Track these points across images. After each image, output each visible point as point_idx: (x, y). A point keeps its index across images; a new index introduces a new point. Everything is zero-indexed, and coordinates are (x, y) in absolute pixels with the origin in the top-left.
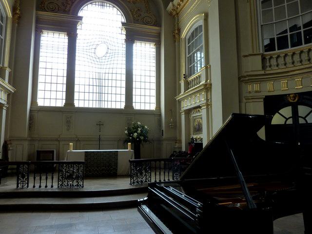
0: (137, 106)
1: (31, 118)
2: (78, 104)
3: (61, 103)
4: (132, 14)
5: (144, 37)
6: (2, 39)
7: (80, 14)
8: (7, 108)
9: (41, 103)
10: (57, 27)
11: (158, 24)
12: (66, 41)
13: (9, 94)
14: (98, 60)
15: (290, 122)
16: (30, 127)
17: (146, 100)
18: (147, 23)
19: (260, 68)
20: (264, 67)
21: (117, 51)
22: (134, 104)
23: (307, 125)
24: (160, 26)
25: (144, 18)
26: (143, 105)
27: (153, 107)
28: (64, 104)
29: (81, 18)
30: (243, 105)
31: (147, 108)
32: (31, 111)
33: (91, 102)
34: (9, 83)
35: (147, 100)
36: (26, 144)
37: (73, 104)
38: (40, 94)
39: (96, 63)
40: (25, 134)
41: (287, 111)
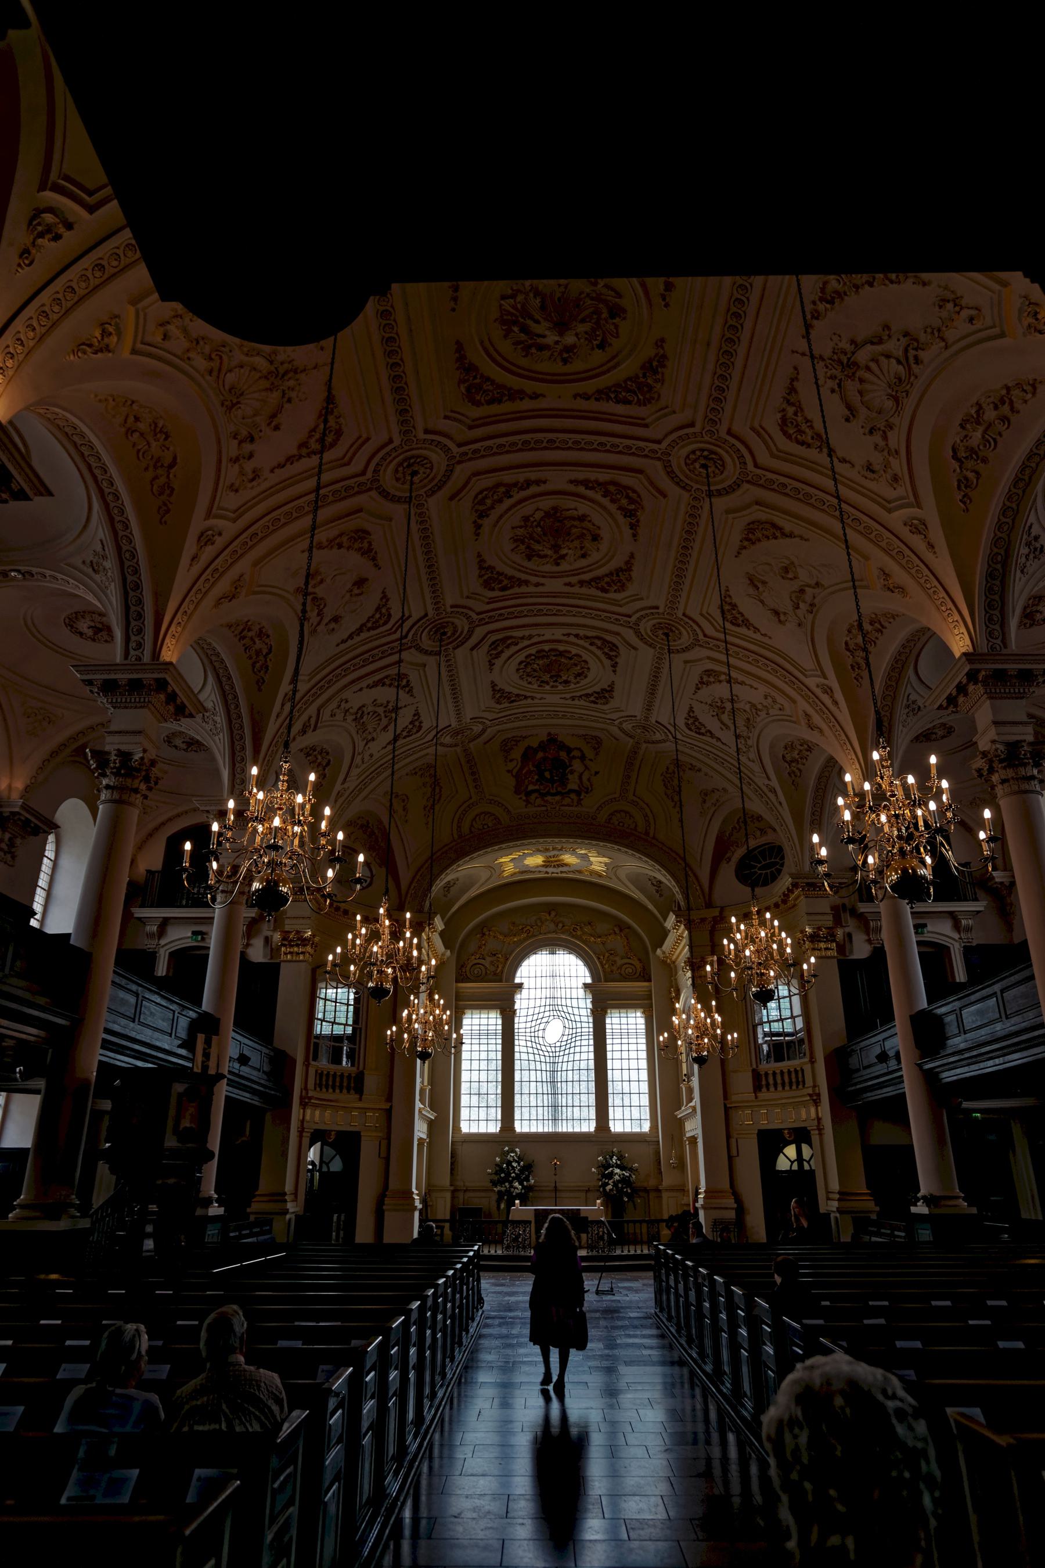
0: (616, 1127)
3: (494, 1128)
4: (601, 963)
5: (625, 1003)
7: (517, 981)
9: (465, 1128)
10: (483, 1003)
11: (645, 976)
12: (500, 1021)
13: (431, 1124)
14: (549, 1049)
15: (795, 1167)
16: (452, 1170)
17: (632, 1114)
18: (625, 978)
19: (751, 1089)
20: (757, 1088)
21: (579, 1030)
23: (812, 1172)
24: (650, 980)
25: (620, 968)
26: (628, 1123)
27: (646, 1127)
28: (498, 1129)
29: (520, 986)
30: (733, 1141)
31: (636, 1130)
33: (540, 1123)
35: (636, 1115)
36: (448, 1195)
37: (513, 1129)
38: (464, 1113)
39: (546, 1054)
40: (446, 1181)
41: (791, 1151)
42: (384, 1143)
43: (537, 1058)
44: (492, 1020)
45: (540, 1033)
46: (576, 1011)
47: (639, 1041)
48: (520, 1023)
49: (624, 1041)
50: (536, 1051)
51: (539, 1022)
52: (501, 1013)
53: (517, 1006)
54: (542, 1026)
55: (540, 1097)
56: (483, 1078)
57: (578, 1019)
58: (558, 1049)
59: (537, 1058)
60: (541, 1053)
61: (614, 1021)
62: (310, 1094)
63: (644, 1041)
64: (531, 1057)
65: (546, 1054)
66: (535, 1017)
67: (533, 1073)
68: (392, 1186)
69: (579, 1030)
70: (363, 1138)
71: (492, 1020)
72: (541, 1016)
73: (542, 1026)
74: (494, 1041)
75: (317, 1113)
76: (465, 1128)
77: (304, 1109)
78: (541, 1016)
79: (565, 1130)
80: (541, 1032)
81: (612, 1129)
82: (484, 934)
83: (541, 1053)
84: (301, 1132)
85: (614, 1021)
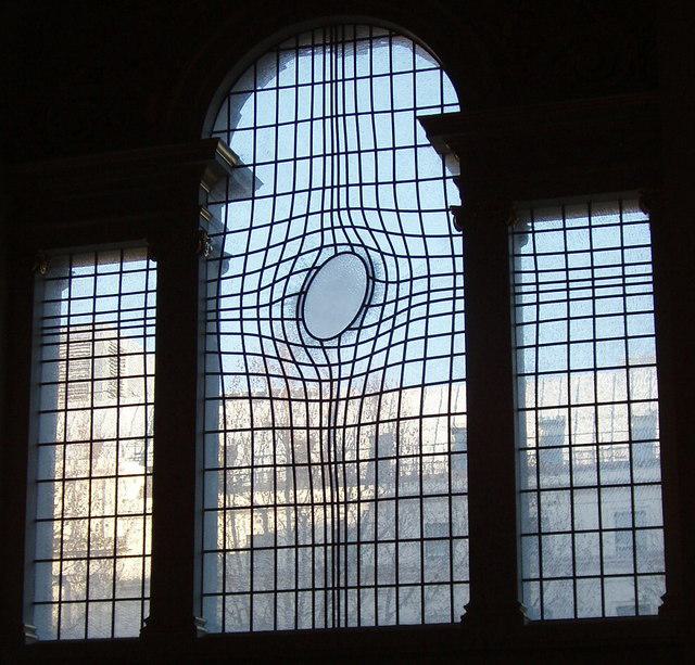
14: (319, 357)
21: (420, 285)
22: (531, 597)
46: (411, 224)
47: (633, 304)
49: (580, 308)
57: (416, 247)
58: (347, 354)
61: (550, 246)
63: (648, 303)
65: (309, 372)
69: (420, 285)
73: (296, 283)
74: (137, 345)
79: (368, 621)
81: (532, 612)
85: (550, 246)
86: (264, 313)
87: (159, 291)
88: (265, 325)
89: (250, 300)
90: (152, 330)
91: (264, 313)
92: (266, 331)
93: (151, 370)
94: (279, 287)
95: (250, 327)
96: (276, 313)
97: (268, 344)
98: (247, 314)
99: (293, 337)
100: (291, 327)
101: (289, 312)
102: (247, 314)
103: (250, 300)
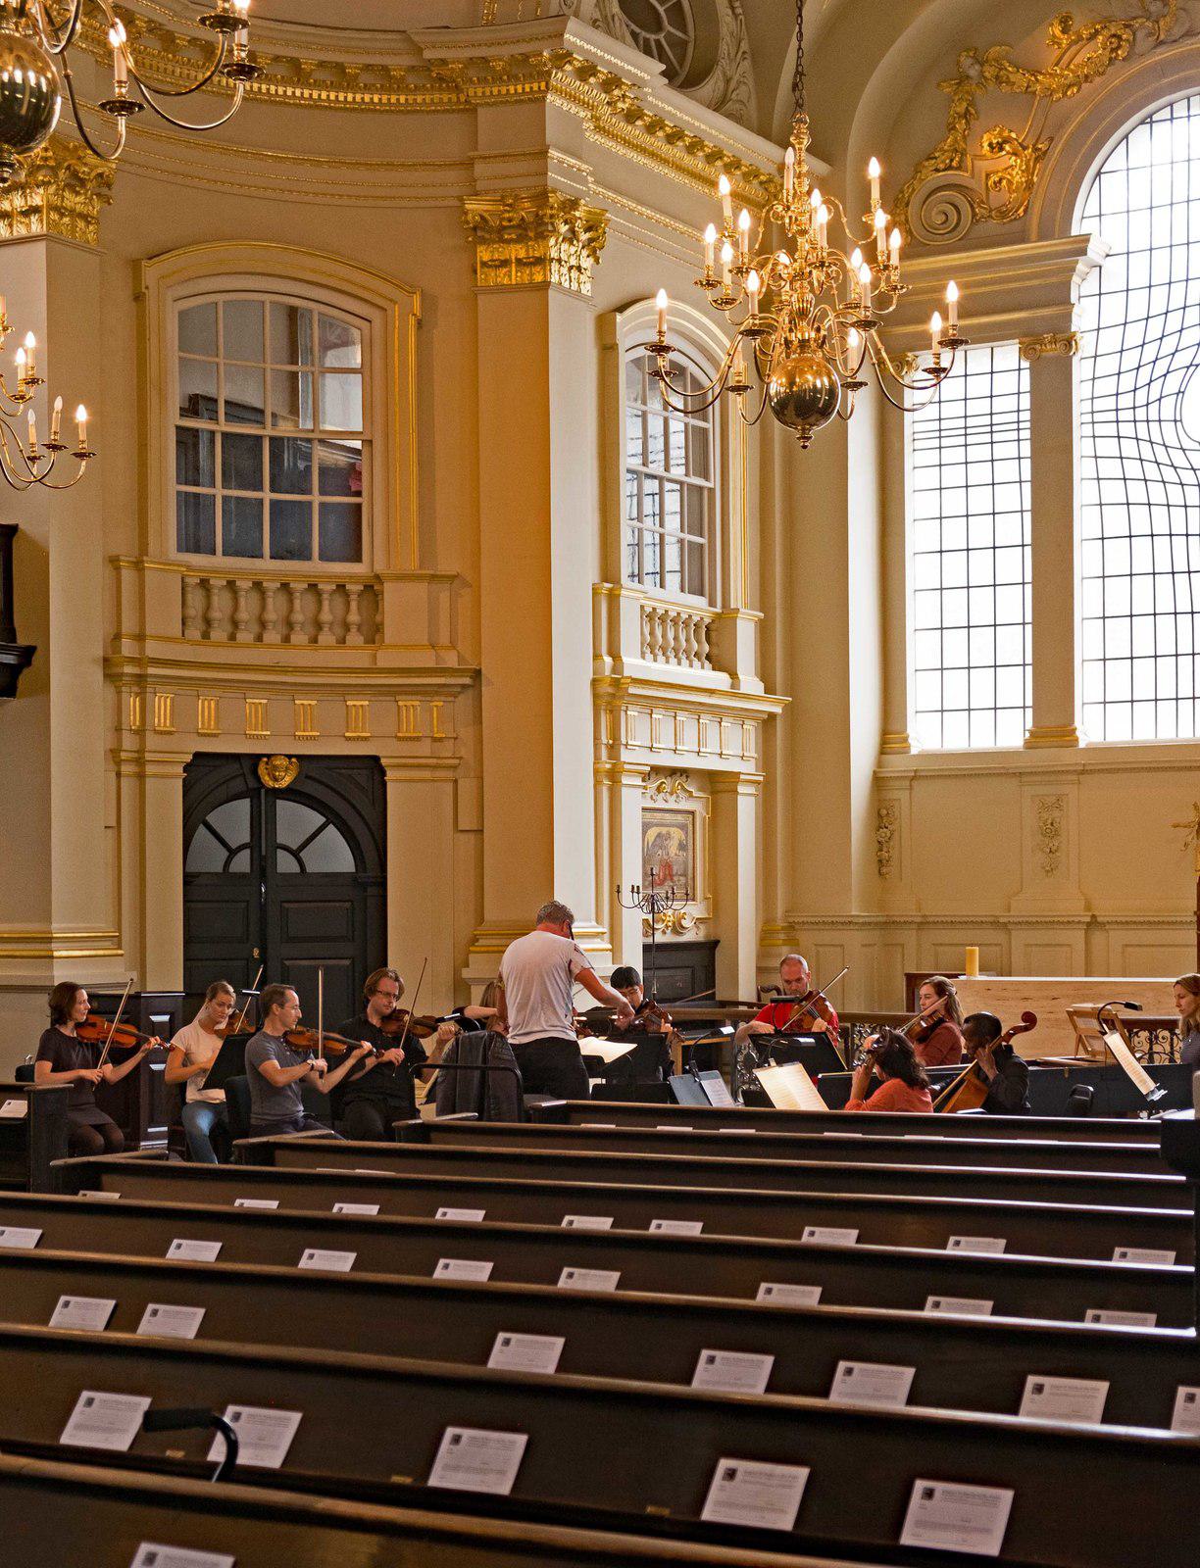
1: (881, 815)
2: (1092, 728)
3: (1012, 733)
6: (711, 491)
8: (766, 790)
9: (924, 736)
32: (879, 782)
34: (765, 674)
38: (920, 691)
42: (467, 786)
43: (1157, 493)
44: (996, 375)
45: (1168, 409)
48: (1091, 383)
50: (1152, 471)
51: (1161, 367)
52: (1025, 352)
53: (1083, 318)
54: (1173, 383)
55: (1165, 623)
56: (981, 573)
59: (1157, 493)
60: (1169, 474)
62: (152, 649)
64: (1137, 492)
66: (1150, 352)
67: (1142, 545)
68: (487, 916)
70: (390, 775)
71: (996, 375)
72: (1169, 344)
73: (1173, 383)
75: (205, 708)
76: (924, 736)
77: (142, 694)
78: (1169, 344)
80: (1168, 404)
82: (963, 79)
83: (1169, 474)
84: (128, 761)
86: (1141, 414)
87: (1033, 392)
88: (1142, 426)
89: (1126, 401)
90: (1026, 434)
91: (1141, 414)
92: (1143, 433)
93: (1027, 475)
94: (1156, 386)
95: (1127, 429)
96: (1153, 416)
97: (1145, 447)
98: (1123, 415)
99: (1171, 441)
100: (1168, 427)
101: (1167, 412)
102: (1123, 415)
103: (1126, 401)
